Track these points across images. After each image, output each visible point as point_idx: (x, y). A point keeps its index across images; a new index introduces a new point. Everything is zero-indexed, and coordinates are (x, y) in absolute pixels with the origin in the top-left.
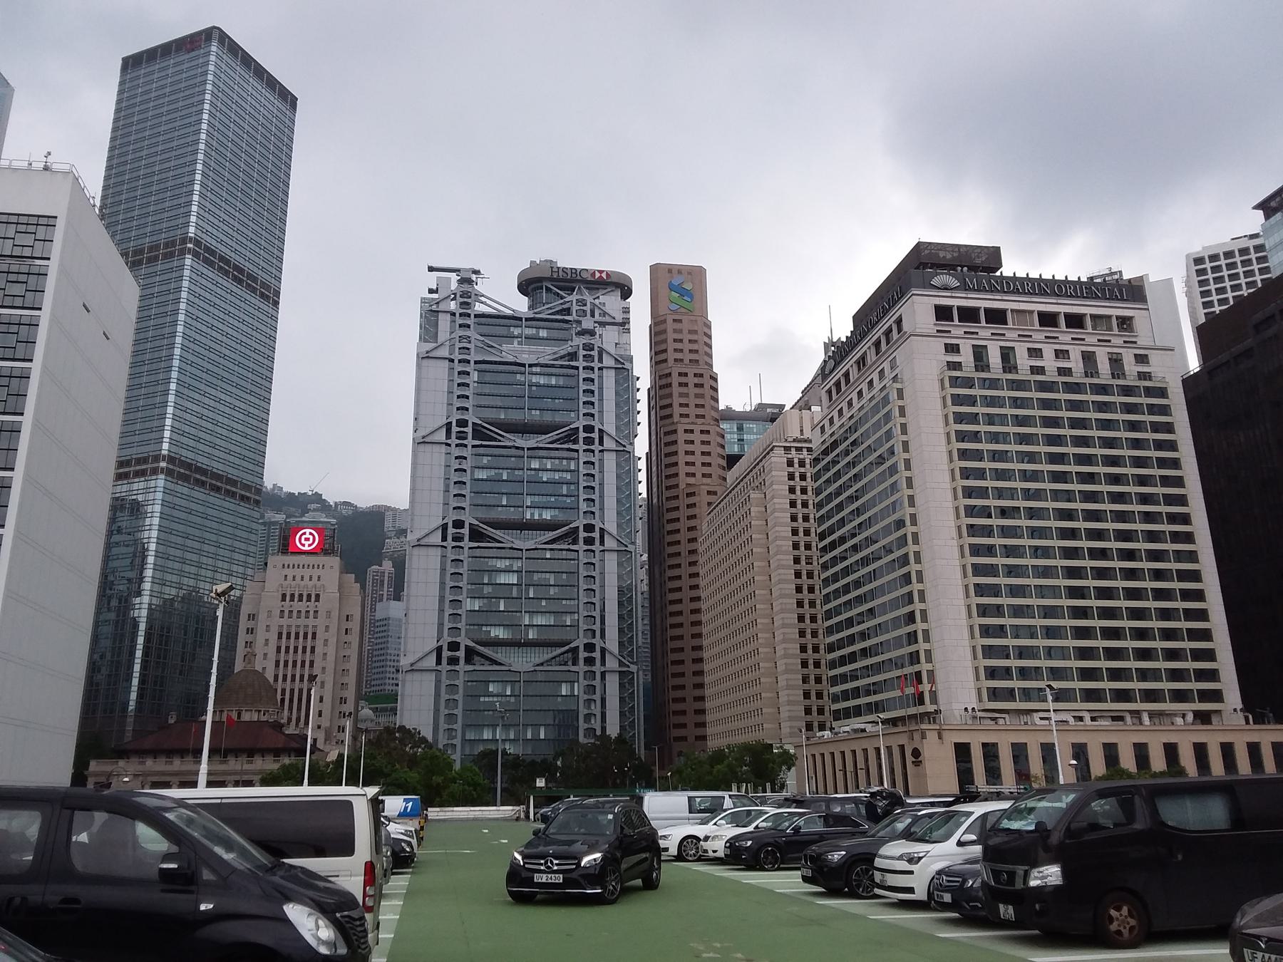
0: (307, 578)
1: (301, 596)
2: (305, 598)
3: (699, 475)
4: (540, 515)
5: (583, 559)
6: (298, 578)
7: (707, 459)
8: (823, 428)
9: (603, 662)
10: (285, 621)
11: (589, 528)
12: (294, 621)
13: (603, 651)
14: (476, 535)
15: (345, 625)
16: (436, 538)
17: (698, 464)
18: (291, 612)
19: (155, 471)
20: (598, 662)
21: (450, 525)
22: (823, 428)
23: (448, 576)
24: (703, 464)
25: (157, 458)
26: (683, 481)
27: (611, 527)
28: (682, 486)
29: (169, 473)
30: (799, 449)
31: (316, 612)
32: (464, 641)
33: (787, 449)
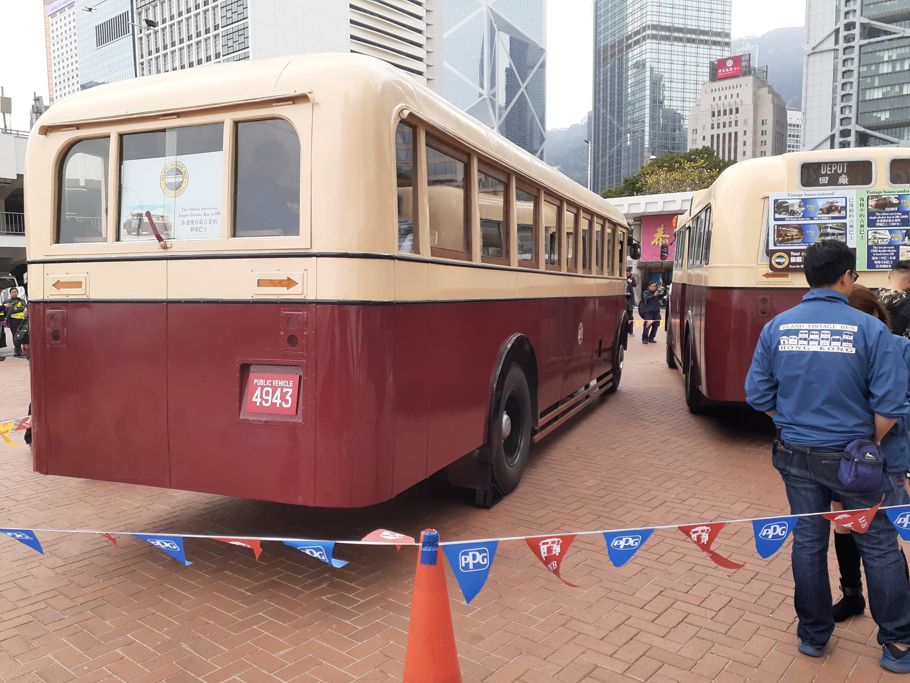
0: (729, 97)
1: (725, 111)
2: (728, 113)
6: (723, 98)
10: (715, 132)
12: (721, 131)
14: (870, 32)
15: (761, 128)
16: (830, 44)
18: (718, 124)
19: (644, 38)
21: (842, 29)
23: (840, 75)
25: (644, 29)
29: (654, 37)
31: (736, 121)
32: (854, 127)
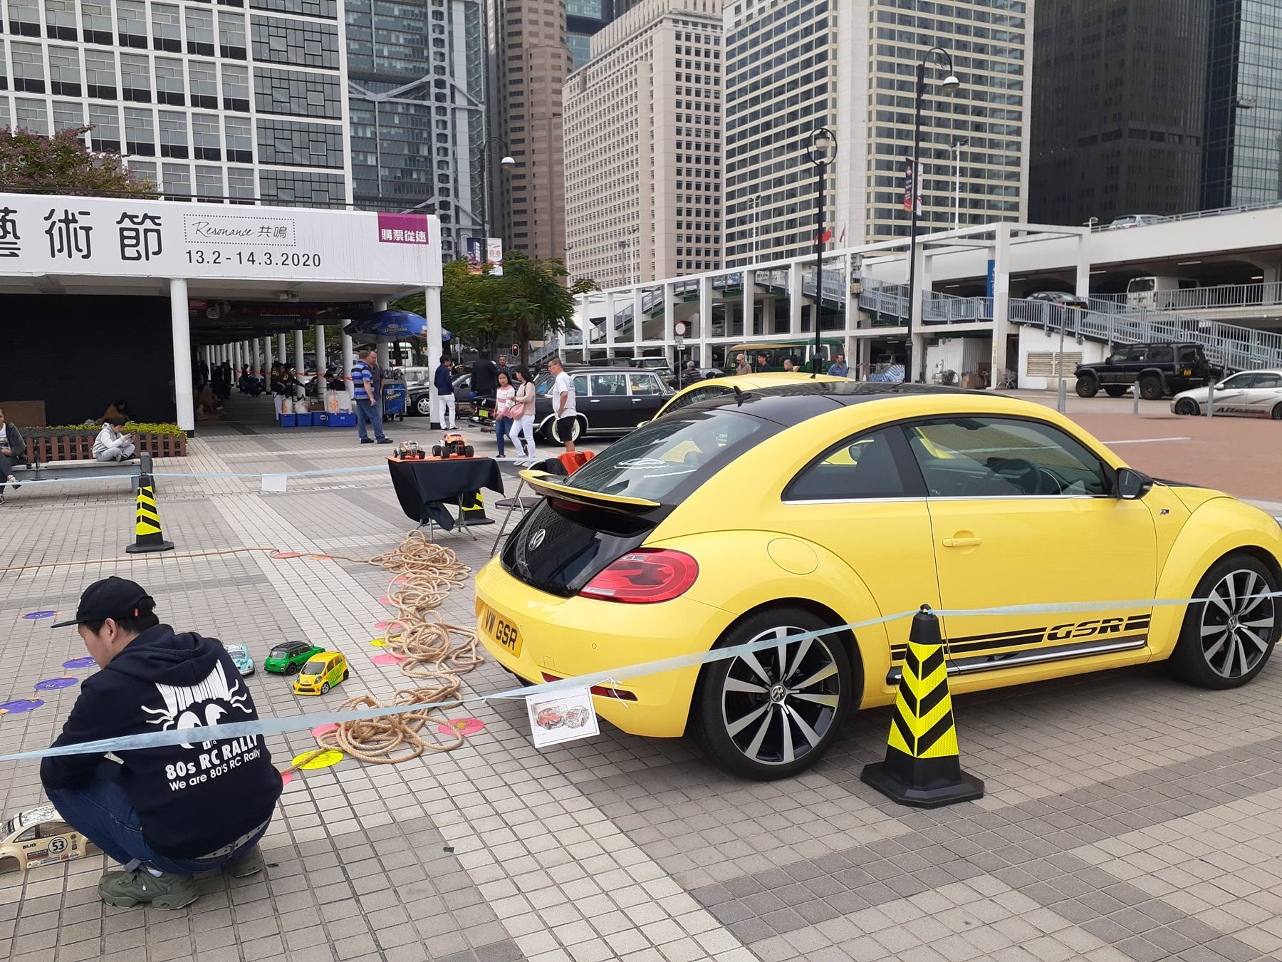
3: (542, 35)
4: (390, 64)
5: (434, 117)
7: (550, 19)
8: (738, 9)
9: (457, 221)
11: (439, 84)
13: (457, 208)
17: (541, 23)
20: (453, 219)
22: (738, 9)
24: (547, 24)
26: (527, 40)
27: (461, 81)
28: (525, 46)
30: (685, 23)
33: (676, 21)
